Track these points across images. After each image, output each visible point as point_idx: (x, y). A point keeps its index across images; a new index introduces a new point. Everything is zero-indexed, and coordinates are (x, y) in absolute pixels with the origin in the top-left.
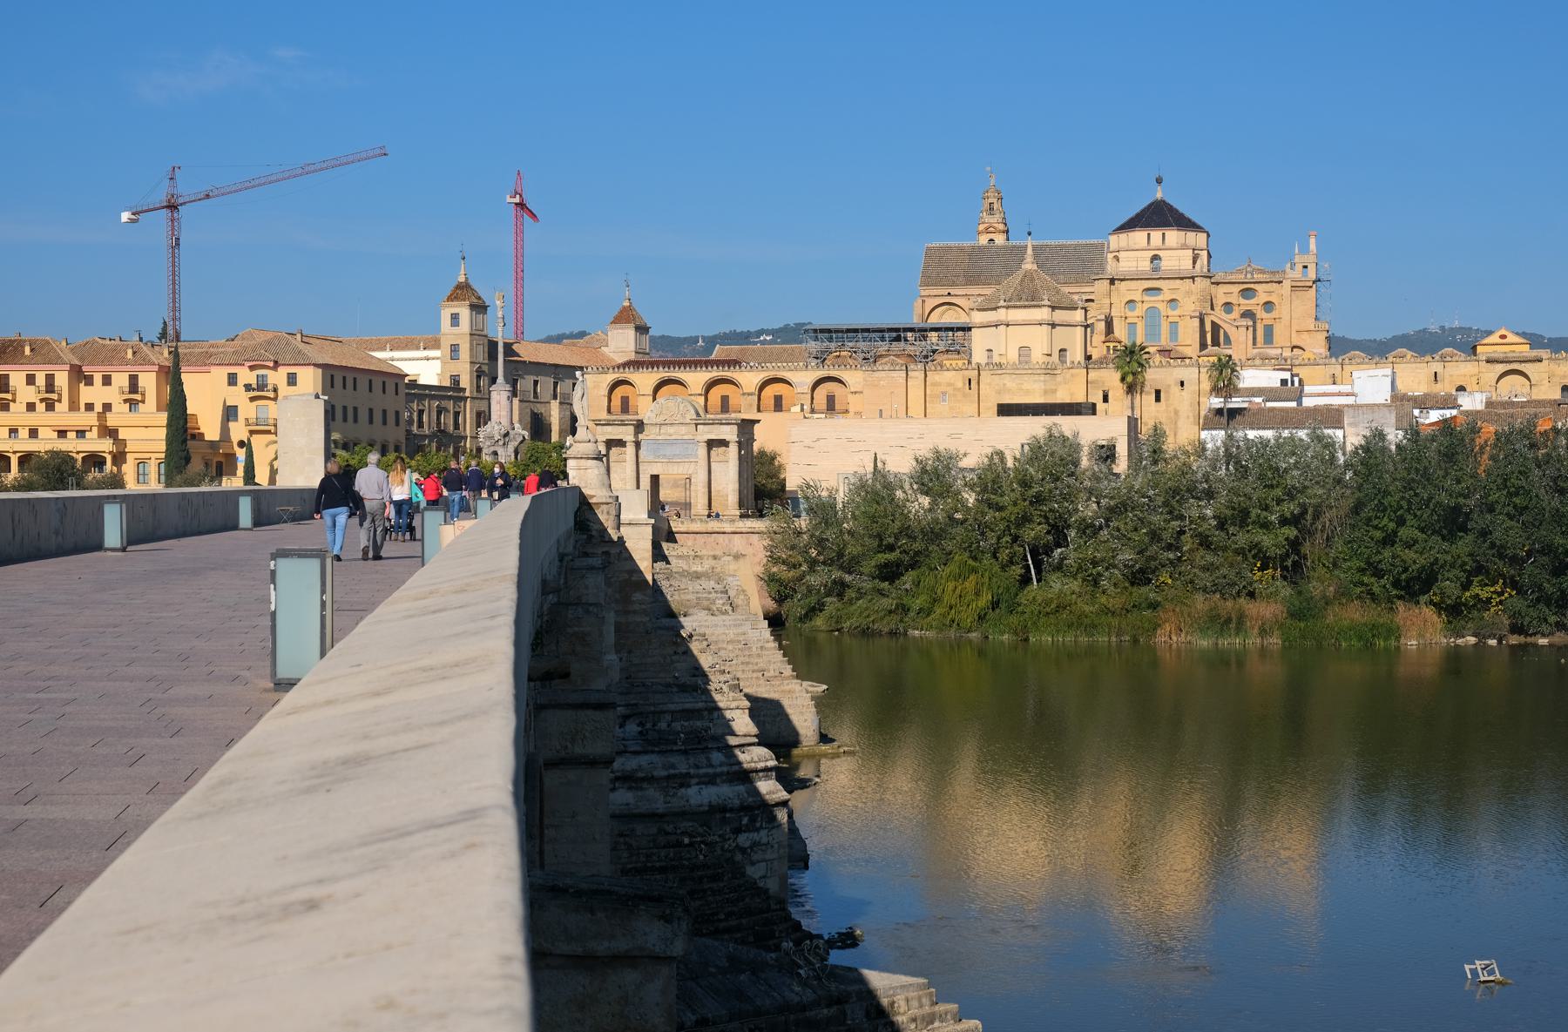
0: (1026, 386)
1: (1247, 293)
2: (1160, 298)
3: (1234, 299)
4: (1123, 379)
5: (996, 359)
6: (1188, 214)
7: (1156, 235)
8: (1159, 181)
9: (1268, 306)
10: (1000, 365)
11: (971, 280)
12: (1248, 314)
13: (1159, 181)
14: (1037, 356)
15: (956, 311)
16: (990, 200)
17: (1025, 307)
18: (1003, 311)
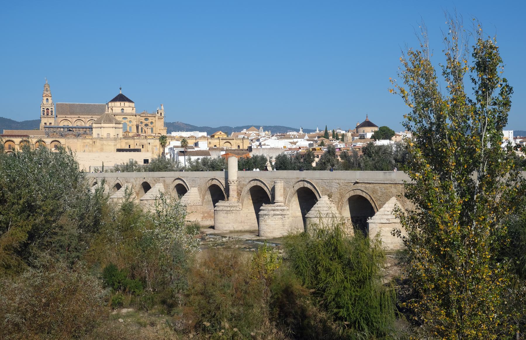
0: (109, 144)
1: (146, 119)
2: (127, 120)
3: (143, 121)
4: (161, 144)
5: (100, 136)
6: (127, 97)
7: (122, 103)
8: (120, 89)
9: (152, 123)
10: (102, 138)
11: (72, 113)
12: (146, 125)
13: (120, 89)
14: (112, 136)
15: (81, 122)
16: (47, 87)
17: (109, 123)
18: (103, 124)
